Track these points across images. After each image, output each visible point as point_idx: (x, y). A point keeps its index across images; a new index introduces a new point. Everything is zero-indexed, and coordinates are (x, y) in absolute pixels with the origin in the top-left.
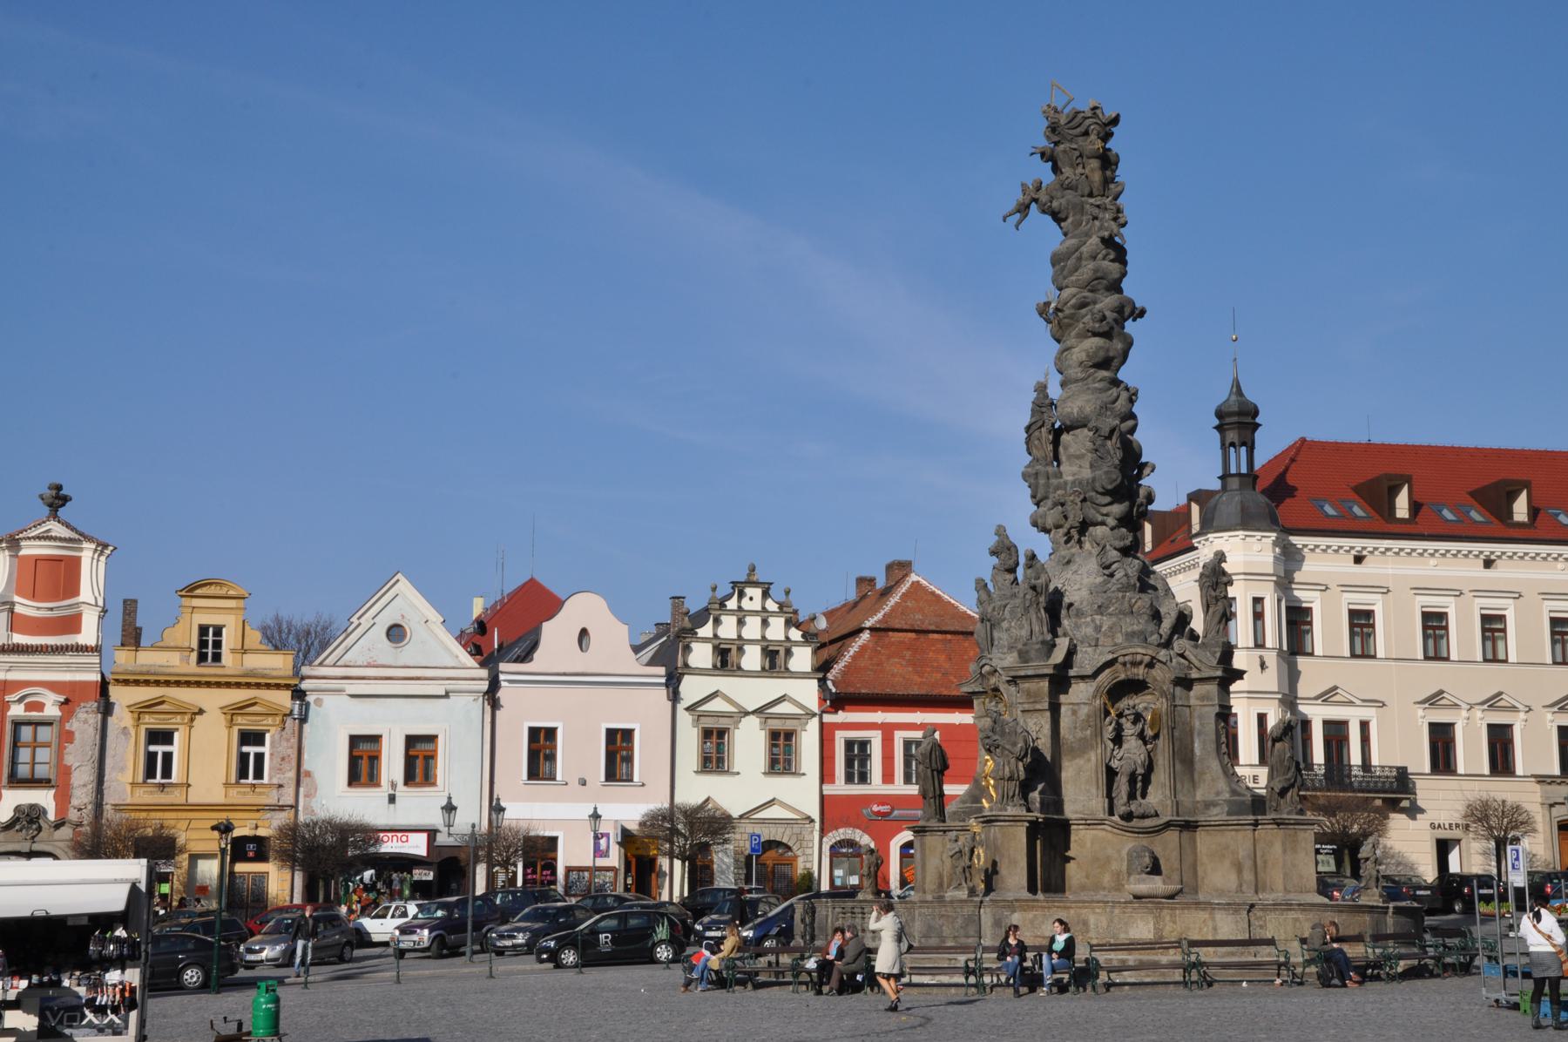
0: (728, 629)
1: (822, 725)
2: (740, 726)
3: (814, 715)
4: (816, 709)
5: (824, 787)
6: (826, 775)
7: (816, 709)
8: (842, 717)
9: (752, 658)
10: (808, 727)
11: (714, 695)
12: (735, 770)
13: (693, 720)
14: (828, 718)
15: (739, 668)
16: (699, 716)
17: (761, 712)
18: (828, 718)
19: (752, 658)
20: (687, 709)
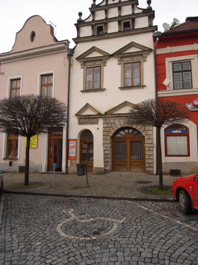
0: (100, 16)
1: (156, 57)
2: (107, 64)
3: (150, 50)
4: (152, 47)
5: (159, 93)
6: (159, 86)
7: (152, 47)
8: (168, 50)
9: (113, 27)
10: (147, 59)
11: (93, 49)
12: (104, 88)
13: (81, 65)
14: (160, 51)
15: (106, 33)
16: (84, 62)
17: (120, 54)
18: (160, 51)
19: (113, 27)
20: (76, 59)
